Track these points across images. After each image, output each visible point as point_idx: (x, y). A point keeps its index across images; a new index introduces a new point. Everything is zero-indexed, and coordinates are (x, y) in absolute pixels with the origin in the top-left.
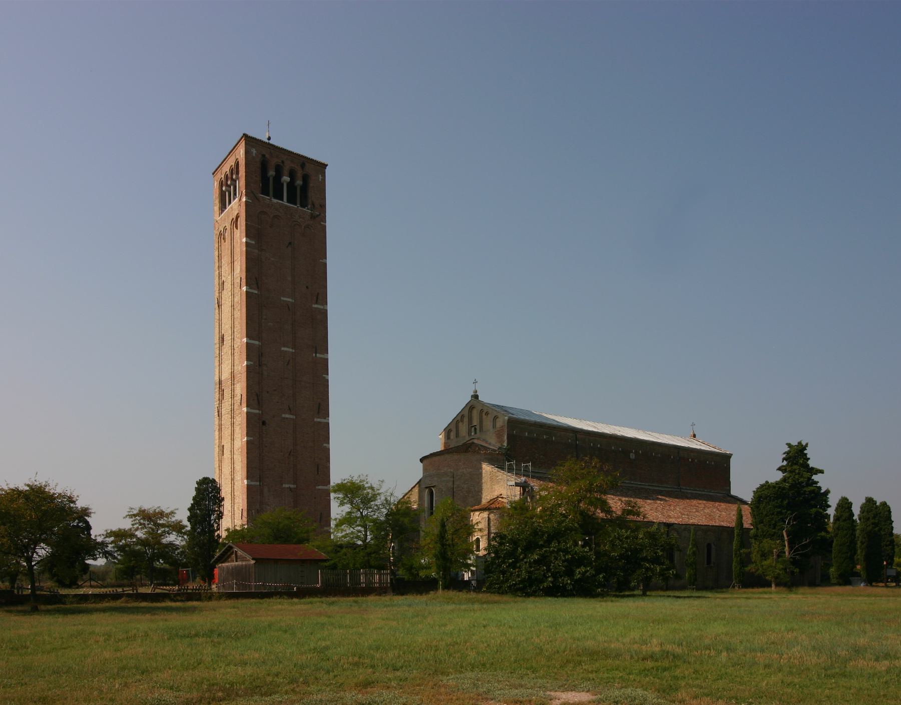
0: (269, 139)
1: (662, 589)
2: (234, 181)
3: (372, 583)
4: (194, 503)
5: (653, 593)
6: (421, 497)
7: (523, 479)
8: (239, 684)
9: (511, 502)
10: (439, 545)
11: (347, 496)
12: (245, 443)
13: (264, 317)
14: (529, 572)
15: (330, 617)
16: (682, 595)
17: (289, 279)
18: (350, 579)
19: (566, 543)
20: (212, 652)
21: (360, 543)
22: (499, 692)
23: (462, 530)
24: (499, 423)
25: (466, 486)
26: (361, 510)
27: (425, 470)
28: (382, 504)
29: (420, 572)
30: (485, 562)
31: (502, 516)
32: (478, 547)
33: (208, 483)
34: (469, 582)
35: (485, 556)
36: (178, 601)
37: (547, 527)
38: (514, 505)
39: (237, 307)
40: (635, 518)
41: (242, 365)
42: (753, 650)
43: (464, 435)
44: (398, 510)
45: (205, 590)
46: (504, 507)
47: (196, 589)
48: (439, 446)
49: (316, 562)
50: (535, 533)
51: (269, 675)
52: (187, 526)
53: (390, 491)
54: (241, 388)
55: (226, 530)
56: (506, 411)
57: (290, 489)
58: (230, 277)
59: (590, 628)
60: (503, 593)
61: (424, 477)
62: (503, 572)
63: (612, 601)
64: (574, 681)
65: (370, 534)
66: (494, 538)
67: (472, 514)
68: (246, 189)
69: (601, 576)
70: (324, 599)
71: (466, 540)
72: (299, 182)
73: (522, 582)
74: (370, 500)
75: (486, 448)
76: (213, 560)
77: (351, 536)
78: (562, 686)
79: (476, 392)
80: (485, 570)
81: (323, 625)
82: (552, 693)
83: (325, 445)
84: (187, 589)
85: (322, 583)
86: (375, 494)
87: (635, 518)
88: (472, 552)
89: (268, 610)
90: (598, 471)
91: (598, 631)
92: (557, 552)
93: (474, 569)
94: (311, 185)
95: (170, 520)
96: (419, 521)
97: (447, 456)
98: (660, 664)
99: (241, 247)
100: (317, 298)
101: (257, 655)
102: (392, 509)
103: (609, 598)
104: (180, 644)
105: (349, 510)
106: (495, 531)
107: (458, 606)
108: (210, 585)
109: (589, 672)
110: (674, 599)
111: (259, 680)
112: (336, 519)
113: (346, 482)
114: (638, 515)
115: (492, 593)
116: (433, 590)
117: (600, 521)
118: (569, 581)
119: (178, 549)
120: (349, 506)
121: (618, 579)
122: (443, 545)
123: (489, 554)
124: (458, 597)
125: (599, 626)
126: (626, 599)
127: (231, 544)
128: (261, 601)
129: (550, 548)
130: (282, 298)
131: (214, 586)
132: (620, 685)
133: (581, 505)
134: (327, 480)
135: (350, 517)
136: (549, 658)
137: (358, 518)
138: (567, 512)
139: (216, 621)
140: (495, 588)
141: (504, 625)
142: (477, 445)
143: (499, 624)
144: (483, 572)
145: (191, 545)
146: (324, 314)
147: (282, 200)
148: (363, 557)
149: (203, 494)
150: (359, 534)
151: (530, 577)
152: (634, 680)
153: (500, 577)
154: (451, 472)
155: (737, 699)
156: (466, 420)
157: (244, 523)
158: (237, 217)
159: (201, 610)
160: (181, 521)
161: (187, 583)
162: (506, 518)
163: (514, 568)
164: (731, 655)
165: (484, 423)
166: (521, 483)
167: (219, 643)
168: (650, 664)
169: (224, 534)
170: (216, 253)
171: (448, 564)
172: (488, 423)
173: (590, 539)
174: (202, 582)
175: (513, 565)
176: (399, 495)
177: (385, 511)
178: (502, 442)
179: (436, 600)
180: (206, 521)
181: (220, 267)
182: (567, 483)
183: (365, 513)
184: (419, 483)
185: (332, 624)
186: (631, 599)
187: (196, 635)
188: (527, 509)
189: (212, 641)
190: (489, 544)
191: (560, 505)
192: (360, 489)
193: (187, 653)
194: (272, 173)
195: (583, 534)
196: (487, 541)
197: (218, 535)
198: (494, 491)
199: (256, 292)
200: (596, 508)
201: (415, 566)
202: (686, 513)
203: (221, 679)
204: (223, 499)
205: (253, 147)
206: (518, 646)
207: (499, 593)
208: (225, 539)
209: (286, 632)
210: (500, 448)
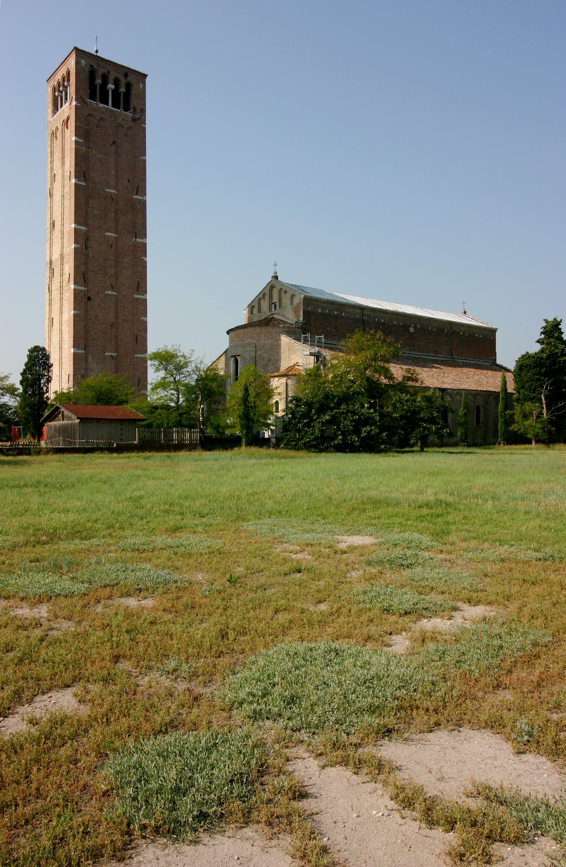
0: (97, 52)
1: (437, 446)
2: (65, 87)
3: (183, 440)
4: (26, 368)
5: (430, 449)
6: (227, 365)
7: (317, 349)
8: (62, 529)
9: (306, 369)
10: (242, 407)
11: (161, 363)
12: (72, 316)
13: (91, 206)
14: (322, 431)
15: (145, 470)
16: (454, 451)
17: (113, 173)
18: (164, 436)
19: (354, 405)
20: (38, 500)
21: (173, 404)
22: (293, 536)
23: (263, 394)
24: (297, 300)
25: (266, 355)
26: (174, 376)
27: (231, 341)
28: (193, 371)
29: (226, 430)
30: (283, 422)
31: (298, 382)
32: (277, 409)
33: (39, 351)
34: (268, 440)
35: (283, 416)
36: (10, 455)
37: (338, 391)
38: (308, 372)
39: (67, 197)
40: (413, 384)
41: (70, 247)
42: (515, 499)
43: (265, 310)
44: (207, 376)
45: (34, 445)
46: (300, 374)
47: (26, 445)
48: (244, 321)
49: (134, 421)
50: (327, 396)
51: (88, 521)
52: (19, 389)
53: (200, 359)
54: (69, 268)
55: (54, 393)
56: (302, 290)
57: (112, 356)
58: (60, 171)
59: (374, 480)
60: (298, 449)
61: (231, 347)
62: (299, 431)
63: (394, 456)
64: (359, 527)
65: (182, 397)
66: (291, 401)
67: (272, 379)
68: (76, 94)
69: (384, 434)
70: (140, 454)
71: (266, 403)
72: (123, 90)
73: (316, 439)
74: (182, 367)
75: (284, 322)
76: (42, 419)
77: (166, 399)
78: (348, 531)
79: (276, 273)
80: (283, 429)
81: (139, 476)
82: (340, 537)
83: (143, 318)
84: (19, 445)
85: (139, 440)
86: (186, 362)
87: (413, 384)
88: (272, 413)
89: (91, 464)
90: (382, 343)
91: (381, 482)
92: (346, 414)
93: (273, 428)
94: (133, 92)
95: (4, 383)
96: (225, 386)
97: (250, 329)
98: (434, 511)
99: (71, 144)
100: (137, 190)
101: (78, 504)
102: (201, 375)
103: (391, 454)
104: (10, 494)
105: (164, 376)
106: (292, 395)
107: (259, 461)
108: (39, 441)
109: (372, 518)
110: (448, 454)
111: (80, 526)
112: (152, 384)
113: (161, 351)
114: (417, 381)
115: (289, 449)
116: (237, 447)
117: (383, 386)
118: (356, 439)
119: (11, 409)
120: (163, 372)
121: (399, 437)
122: (246, 407)
123: (287, 415)
124: (259, 452)
125: (381, 478)
126: (406, 454)
127: (58, 405)
128: (85, 455)
129: (339, 409)
130: (106, 190)
131: (42, 442)
132: (399, 529)
133: (367, 372)
134: (144, 349)
135: (165, 382)
136: (337, 506)
137: (172, 382)
138: (355, 379)
139: (43, 473)
140: (292, 445)
141: (299, 477)
142: (277, 320)
143: (294, 476)
144: (282, 430)
145: (22, 406)
146: (144, 204)
147: (108, 105)
148: (176, 417)
149: (34, 361)
150: (172, 397)
151: (322, 435)
152: (412, 525)
153: (296, 435)
154: (254, 343)
155: (500, 542)
156: (267, 297)
157: (70, 387)
158: (68, 119)
159: (30, 463)
160: (14, 385)
161: (19, 439)
162: (303, 384)
163: (309, 427)
164: (496, 503)
165: (283, 301)
166: (315, 353)
167: (45, 493)
168: (425, 511)
169: (52, 396)
170: (49, 150)
171: (250, 424)
172: (286, 300)
173: (375, 402)
174: (32, 438)
175: (308, 425)
176: (208, 362)
177: (195, 377)
178: (298, 317)
179: (239, 455)
180: (37, 384)
181: (52, 162)
182: (355, 353)
183: (178, 378)
184: (226, 352)
185: (147, 476)
186: (410, 454)
187: (25, 485)
188: (320, 376)
189: (39, 491)
190: (287, 406)
191: (348, 373)
192: (173, 357)
193: (15, 501)
194: (99, 81)
195: (369, 398)
196: (285, 403)
197: (47, 397)
198: (292, 360)
199: (84, 184)
200: (380, 375)
201: (221, 425)
202: (458, 379)
203: (46, 524)
204: (52, 365)
205: (83, 58)
206: (311, 495)
207: (296, 449)
208: (53, 400)
209: (105, 483)
210: (296, 322)
